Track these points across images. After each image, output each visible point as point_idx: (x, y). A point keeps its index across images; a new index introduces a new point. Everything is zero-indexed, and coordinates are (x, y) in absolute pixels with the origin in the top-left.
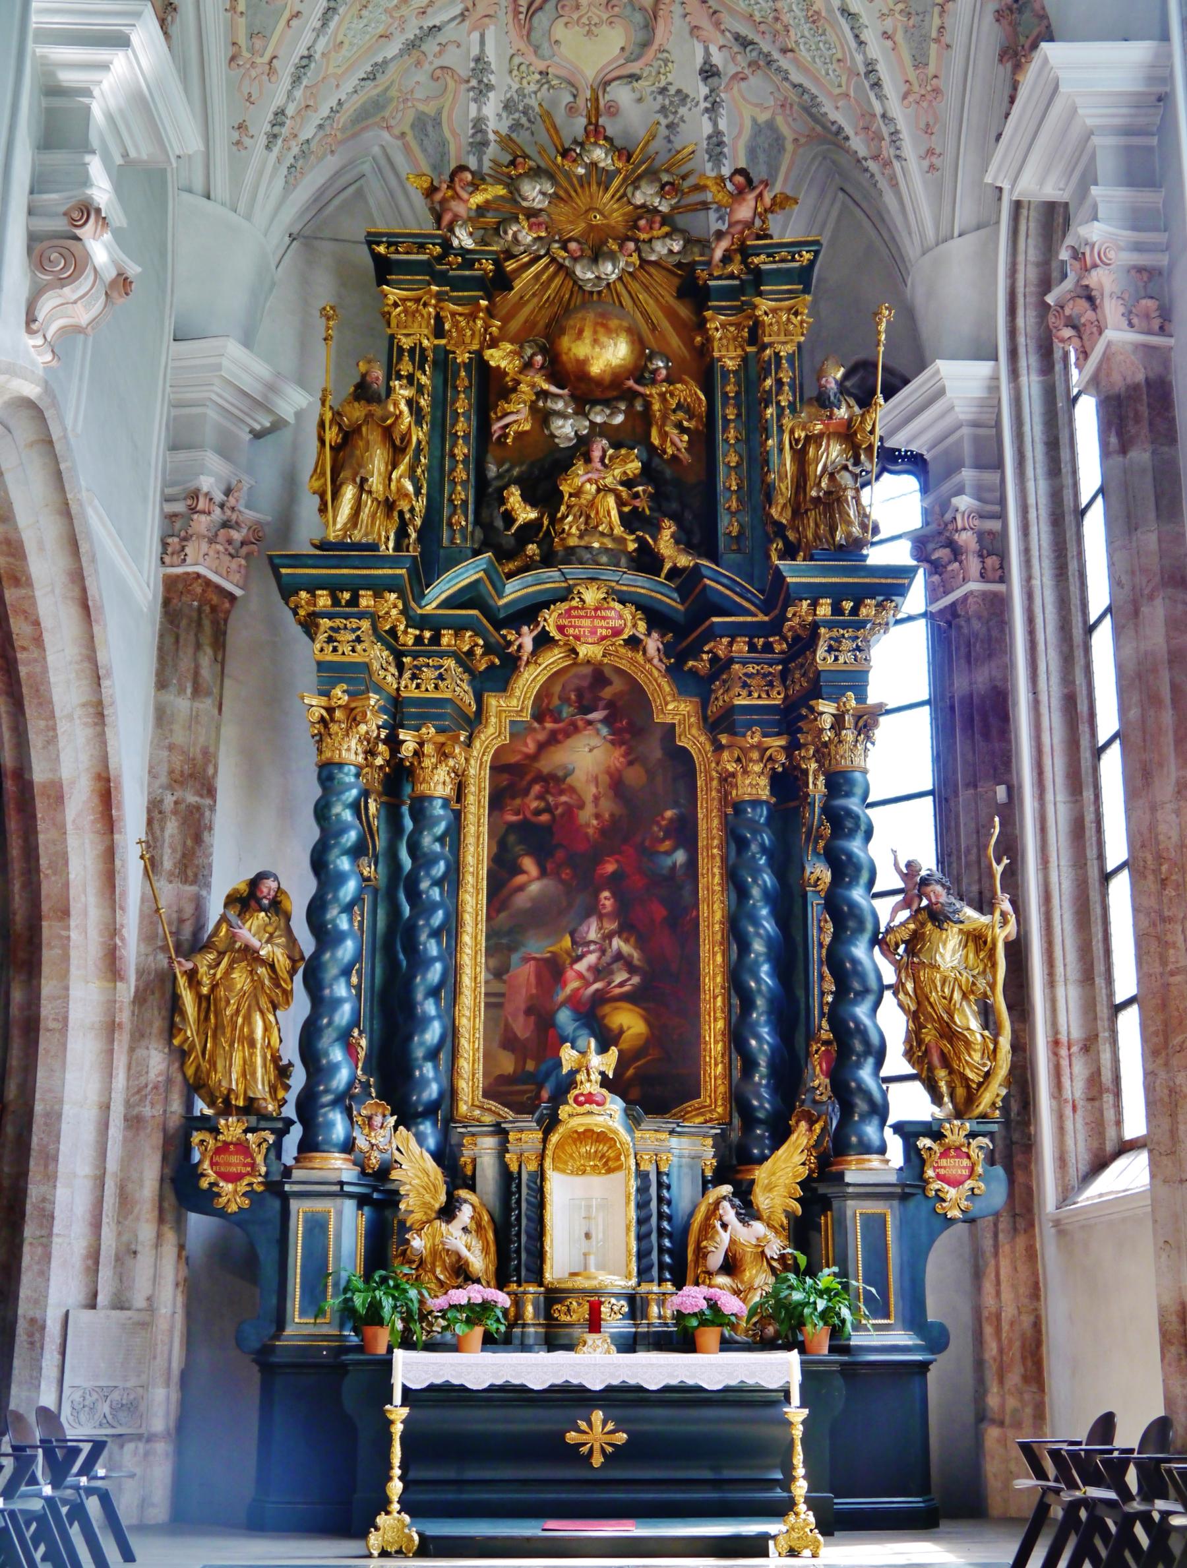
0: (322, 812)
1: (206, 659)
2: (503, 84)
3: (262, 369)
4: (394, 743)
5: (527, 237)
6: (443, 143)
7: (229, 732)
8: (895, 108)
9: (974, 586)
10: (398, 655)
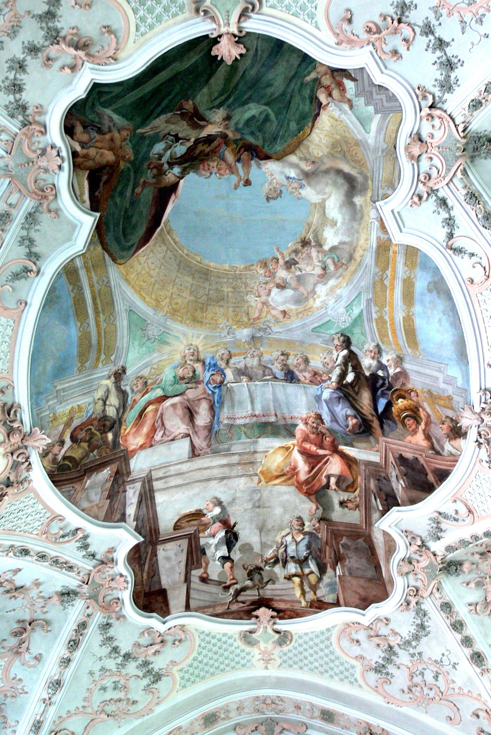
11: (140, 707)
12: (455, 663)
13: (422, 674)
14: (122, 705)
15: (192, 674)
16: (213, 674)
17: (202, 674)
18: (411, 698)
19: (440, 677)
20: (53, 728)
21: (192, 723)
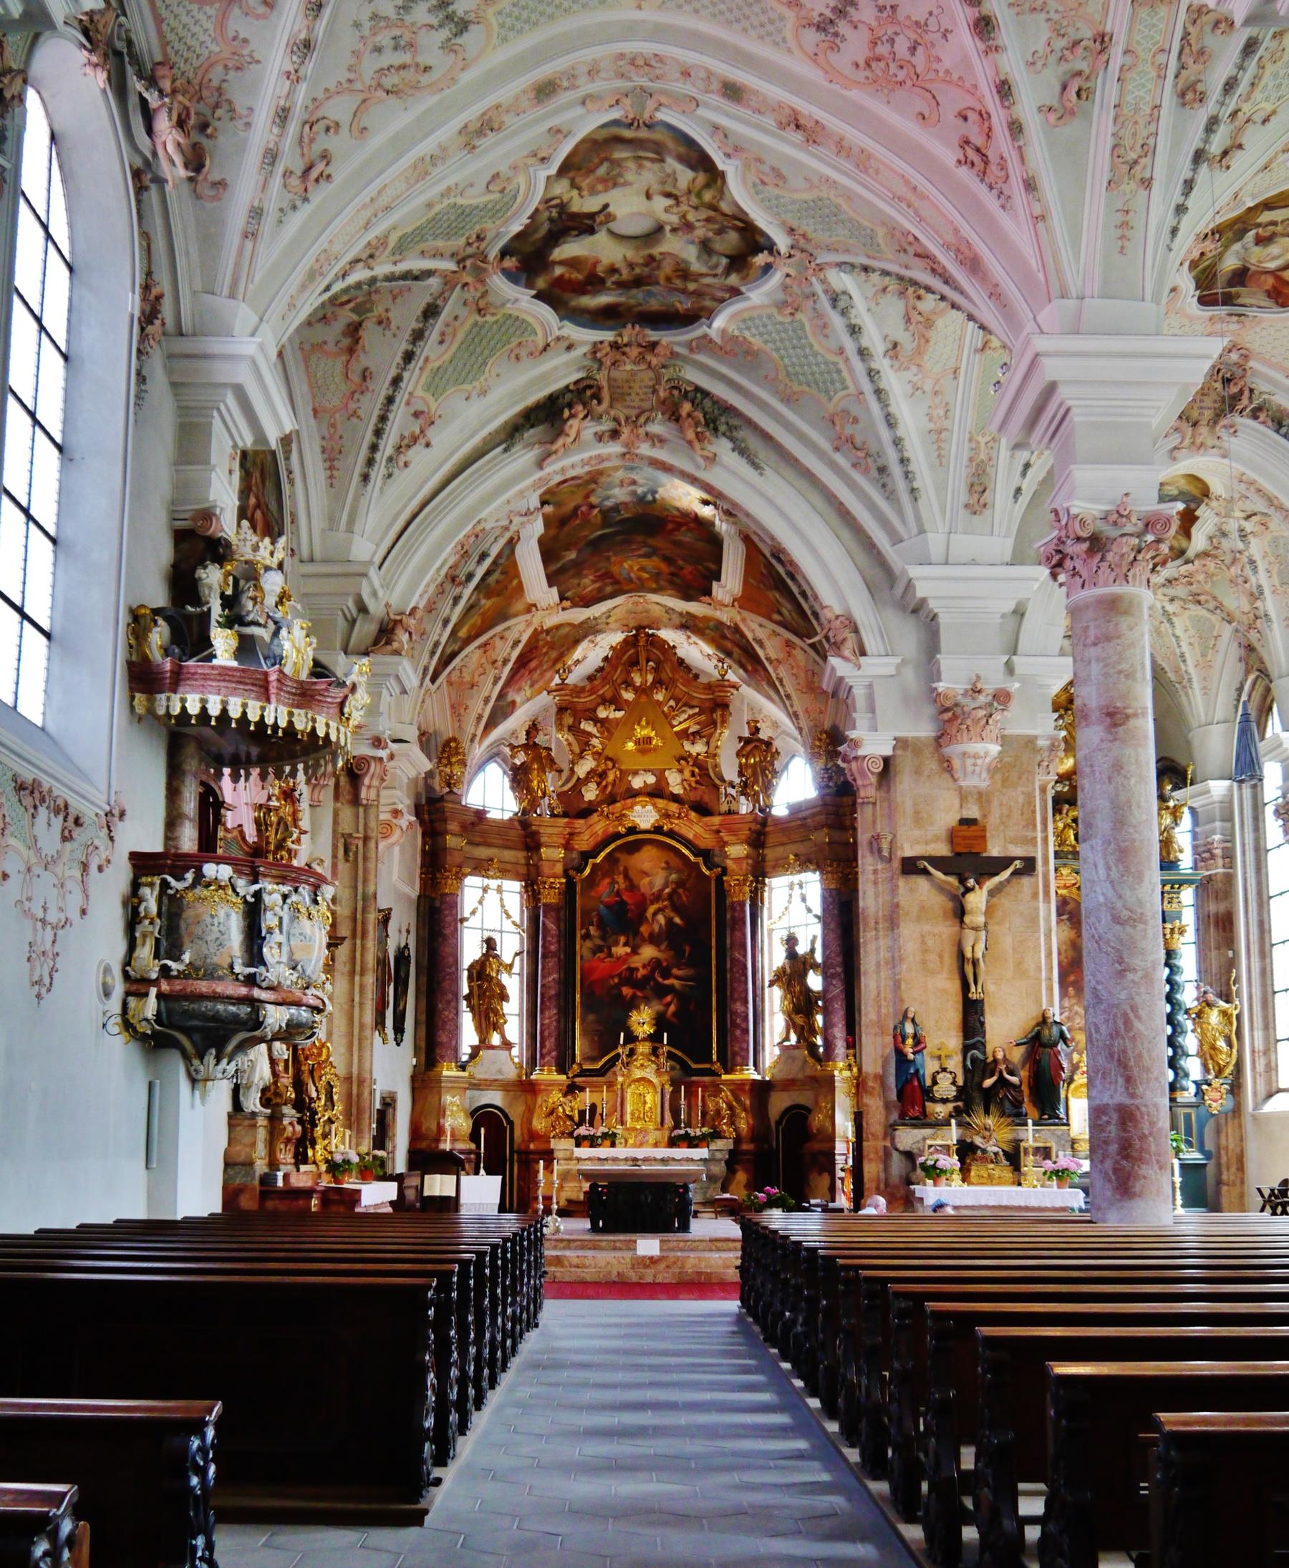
11: (435, 75)
12: (946, 30)
13: (892, 41)
14: (409, 75)
15: (517, 19)
16: (551, 17)
17: (533, 17)
18: (867, 78)
19: (920, 50)
20: (306, 117)
21: (517, 98)
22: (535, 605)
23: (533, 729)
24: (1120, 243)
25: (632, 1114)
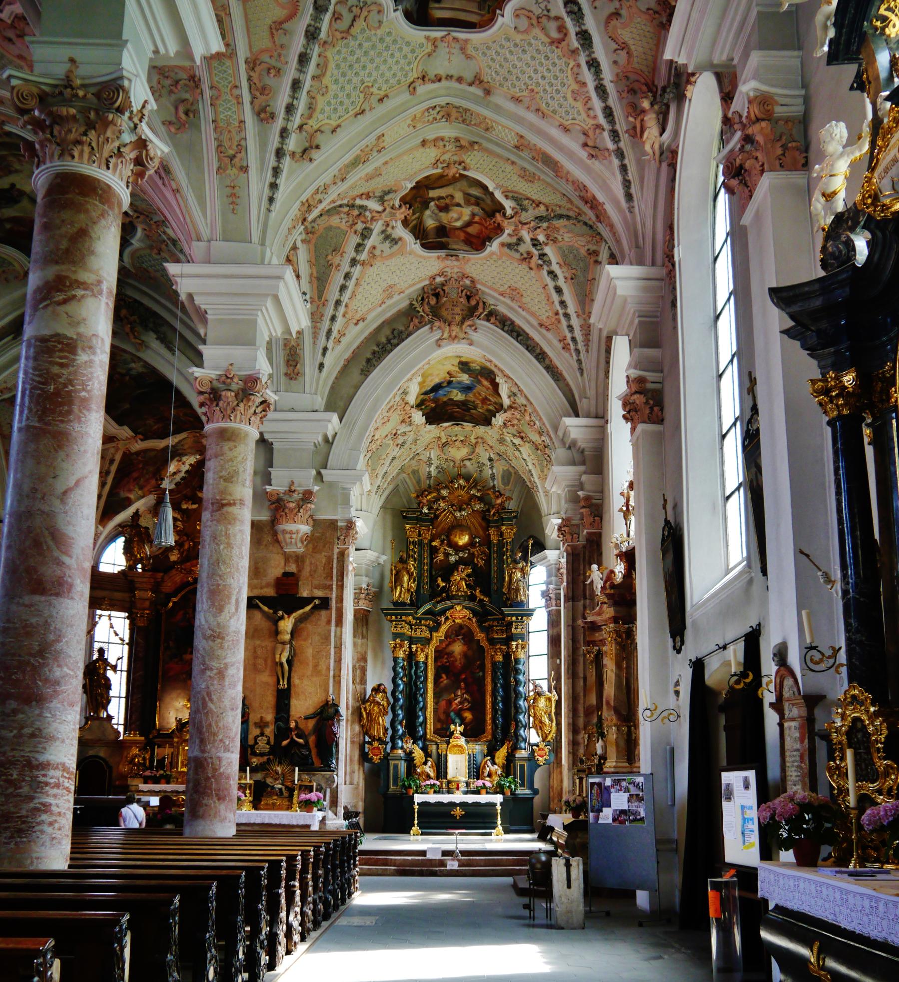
0: (394, 669)
1: (364, 629)
2: (435, 462)
3: (376, 554)
4: (410, 648)
5: (442, 505)
6: (419, 476)
7: (369, 644)
8: (537, 480)
9: (554, 608)
10: (410, 625)
22: (115, 437)
23: (136, 515)
24: (231, 206)
25: (182, 762)
